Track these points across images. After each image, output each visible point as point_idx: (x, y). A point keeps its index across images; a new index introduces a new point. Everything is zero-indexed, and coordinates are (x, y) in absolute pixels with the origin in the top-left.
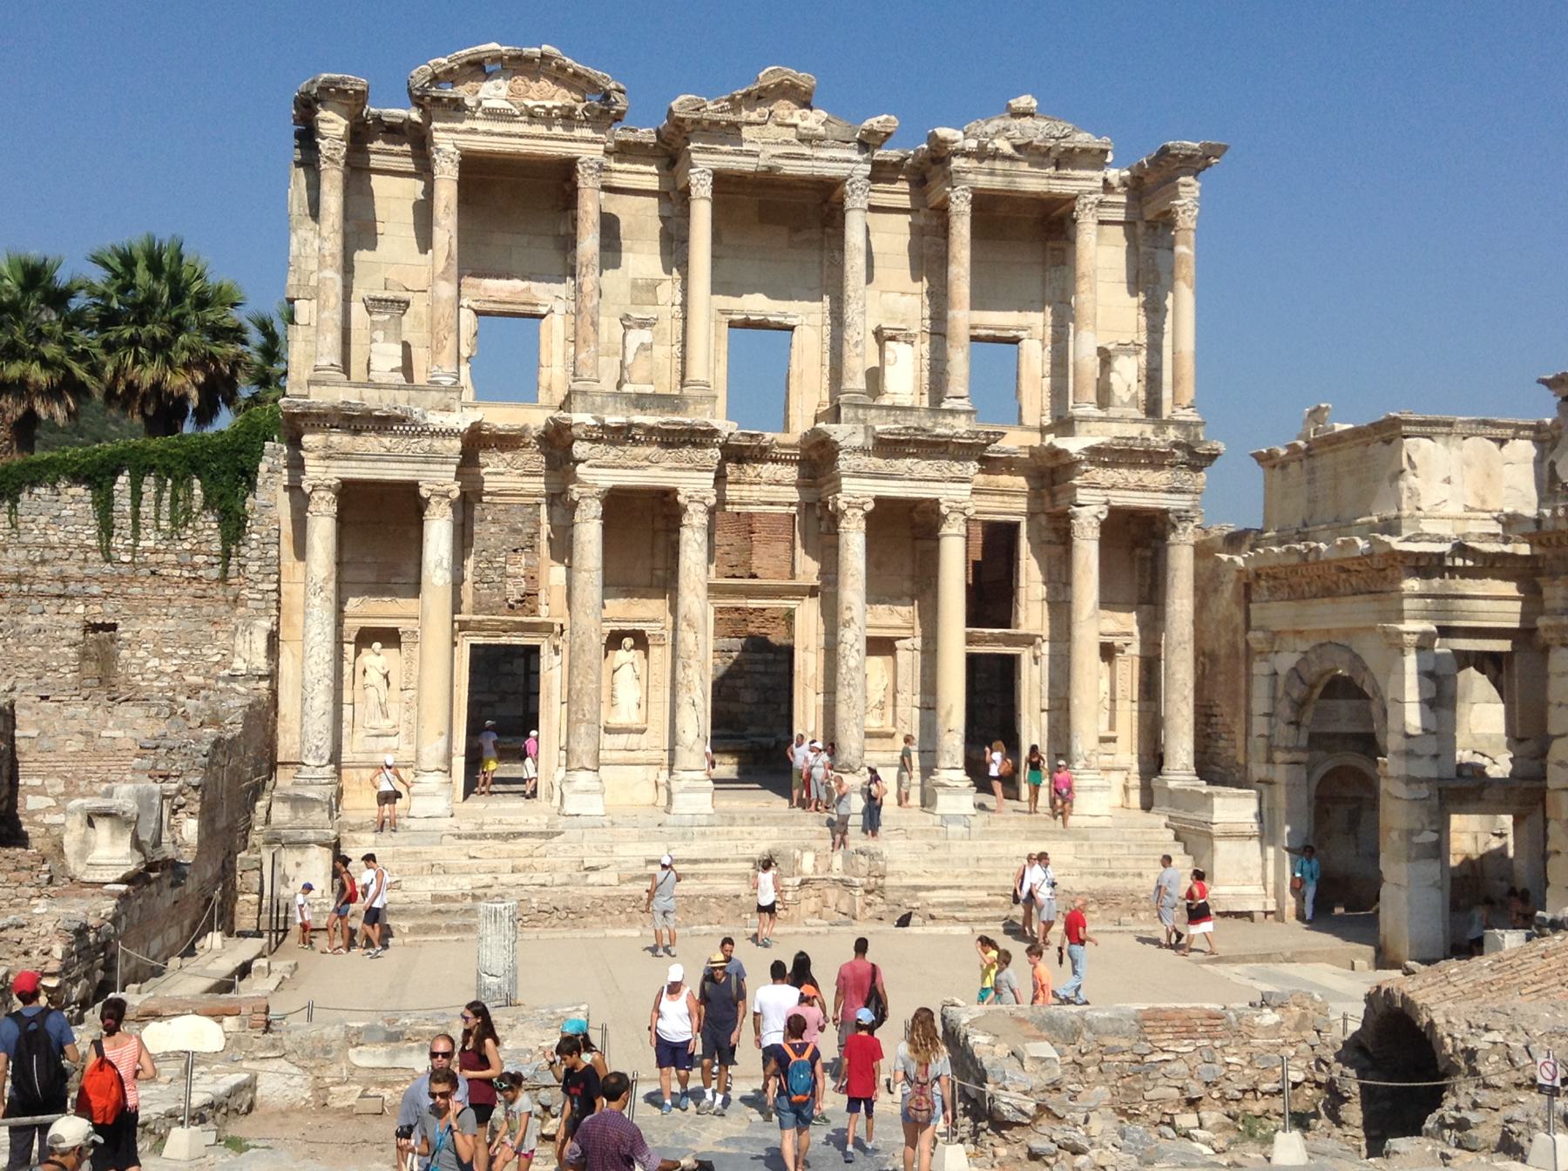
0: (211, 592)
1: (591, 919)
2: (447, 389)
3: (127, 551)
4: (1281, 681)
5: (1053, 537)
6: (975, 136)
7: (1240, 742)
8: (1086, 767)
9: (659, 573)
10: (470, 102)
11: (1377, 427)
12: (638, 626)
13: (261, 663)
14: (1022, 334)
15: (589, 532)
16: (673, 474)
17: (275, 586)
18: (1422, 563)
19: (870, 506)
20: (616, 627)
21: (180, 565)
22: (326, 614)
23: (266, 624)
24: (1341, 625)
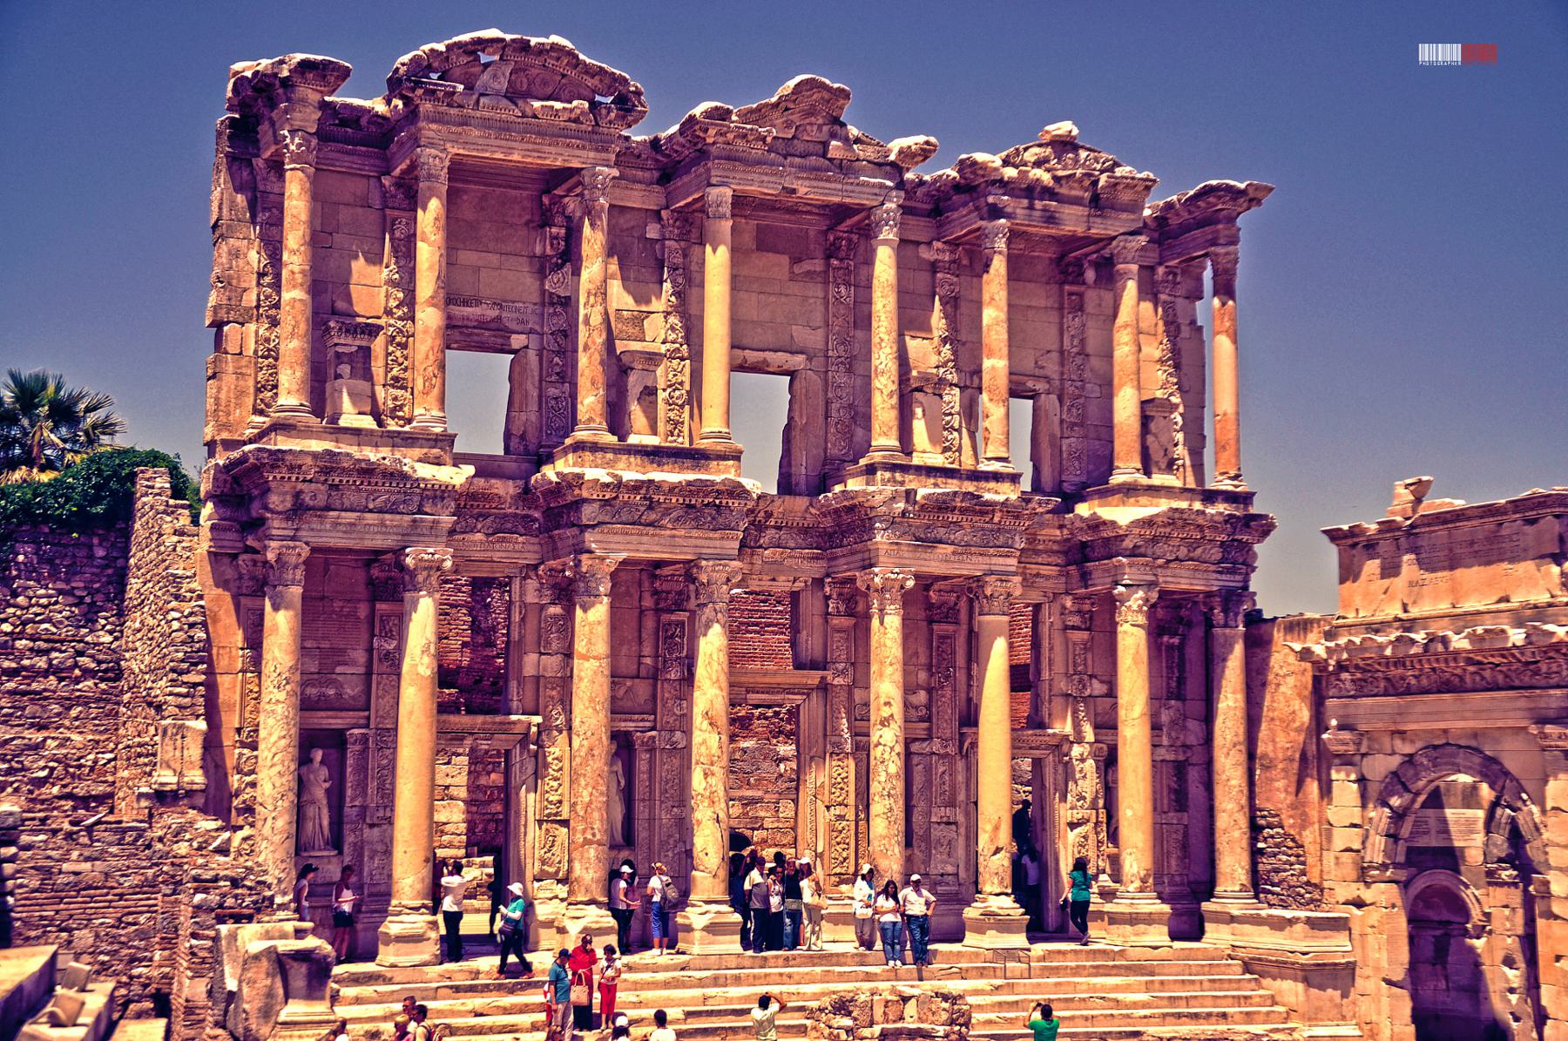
5: (1074, 620)
6: (1016, 167)
9: (648, 661)
14: (1041, 386)
16: (694, 542)
19: (910, 584)
24: (1471, 724)
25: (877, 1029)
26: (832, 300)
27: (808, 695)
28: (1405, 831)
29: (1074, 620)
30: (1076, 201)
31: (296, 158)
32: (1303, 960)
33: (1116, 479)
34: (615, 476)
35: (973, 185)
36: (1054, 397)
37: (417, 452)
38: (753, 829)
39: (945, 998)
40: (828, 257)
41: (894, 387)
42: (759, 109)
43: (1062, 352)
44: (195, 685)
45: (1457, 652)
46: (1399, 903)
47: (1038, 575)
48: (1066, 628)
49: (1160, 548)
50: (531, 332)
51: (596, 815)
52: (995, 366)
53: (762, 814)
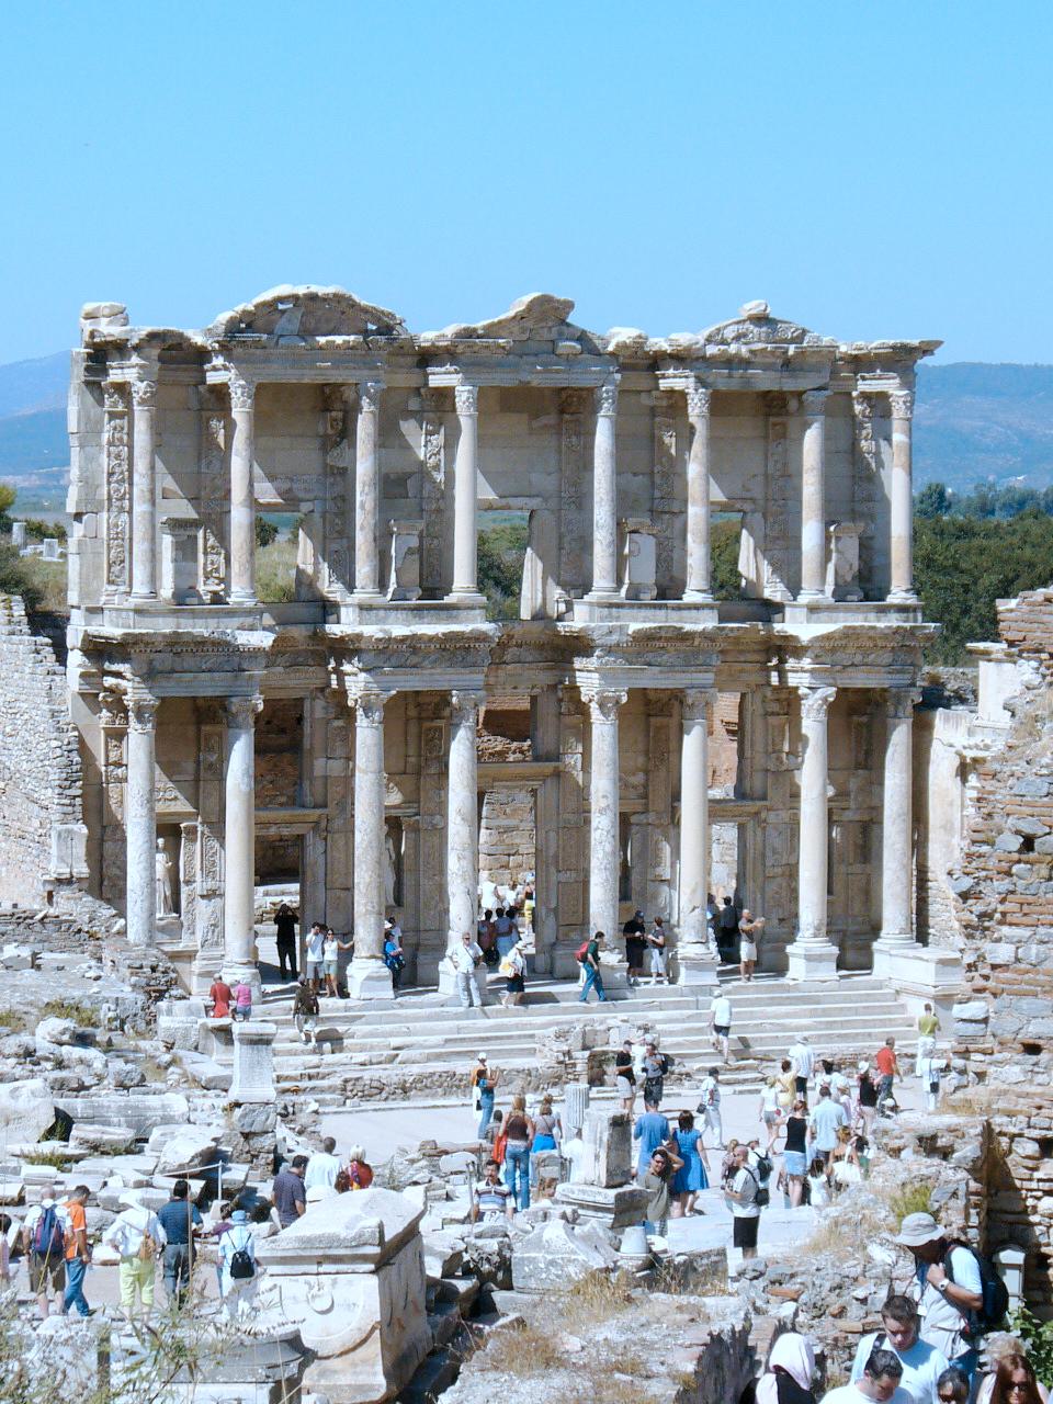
9: (412, 760)
16: (448, 677)
17: (79, 792)
19: (624, 699)
26: (564, 448)
27: (544, 781)
29: (775, 707)
34: (385, 631)
36: (758, 516)
37: (236, 621)
38: (509, 855)
40: (562, 412)
43: (766, 475)
44: (75, 797)
47: (741, 671)
48: (766, 714)
49: (839, 656)
53: (517, 841)
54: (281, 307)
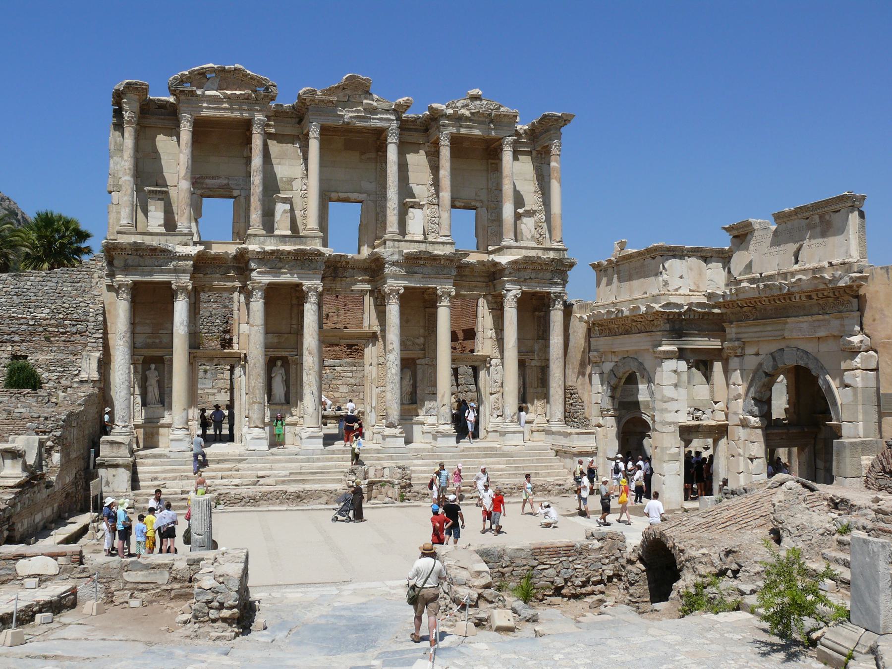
0: (72, 339)
1: (262, 502)
2: (185, 235)
3: (32, 319)
4: (605, 376)
6: (452, 108)
7: (586, 408)
8: (512, 421)
9: (295, 326)
10: (199, 92)
11: (648, 251)
12: (284, 354)
13: (95, 376)
14: (478, 204)
15: (258, 305)
18: (671, 317)
19: (402, 291)
20: (272, 354)
21: (57, 326)
22: (126, 349)
23: (97, 354)
25: (366, 482)
28: (618, 395)
30: (483, 123)
31: (129, 122)
32: (574, 450)
33: (504, 243)
35: (435, 117)
36: (484, 209)
39: (399, 468)
41: (396, 206)
42: (330, 89)
45: (627, 317)
46: (615, 425)
49: (522, 274)
50: (242, 189)
51: (257, 391)
52: (446, 196)
54: (208, 76)
